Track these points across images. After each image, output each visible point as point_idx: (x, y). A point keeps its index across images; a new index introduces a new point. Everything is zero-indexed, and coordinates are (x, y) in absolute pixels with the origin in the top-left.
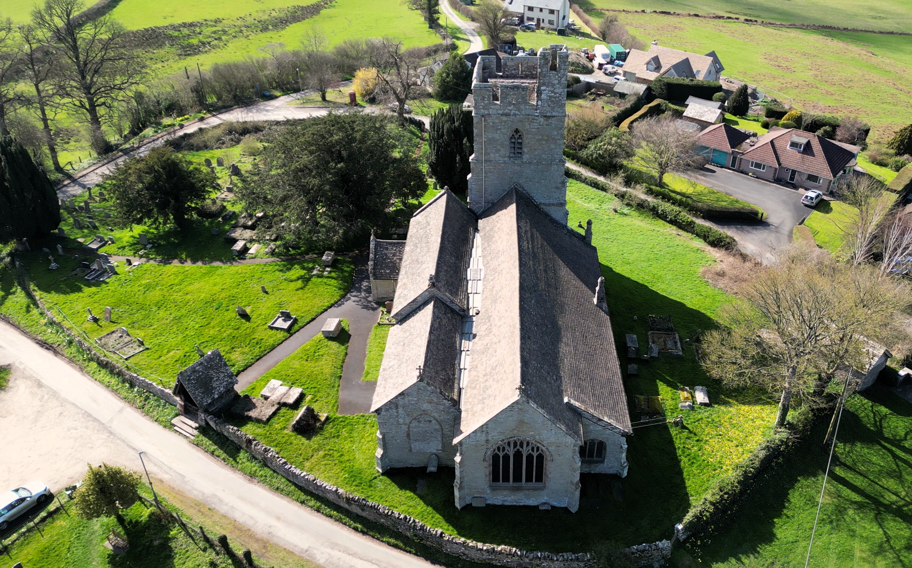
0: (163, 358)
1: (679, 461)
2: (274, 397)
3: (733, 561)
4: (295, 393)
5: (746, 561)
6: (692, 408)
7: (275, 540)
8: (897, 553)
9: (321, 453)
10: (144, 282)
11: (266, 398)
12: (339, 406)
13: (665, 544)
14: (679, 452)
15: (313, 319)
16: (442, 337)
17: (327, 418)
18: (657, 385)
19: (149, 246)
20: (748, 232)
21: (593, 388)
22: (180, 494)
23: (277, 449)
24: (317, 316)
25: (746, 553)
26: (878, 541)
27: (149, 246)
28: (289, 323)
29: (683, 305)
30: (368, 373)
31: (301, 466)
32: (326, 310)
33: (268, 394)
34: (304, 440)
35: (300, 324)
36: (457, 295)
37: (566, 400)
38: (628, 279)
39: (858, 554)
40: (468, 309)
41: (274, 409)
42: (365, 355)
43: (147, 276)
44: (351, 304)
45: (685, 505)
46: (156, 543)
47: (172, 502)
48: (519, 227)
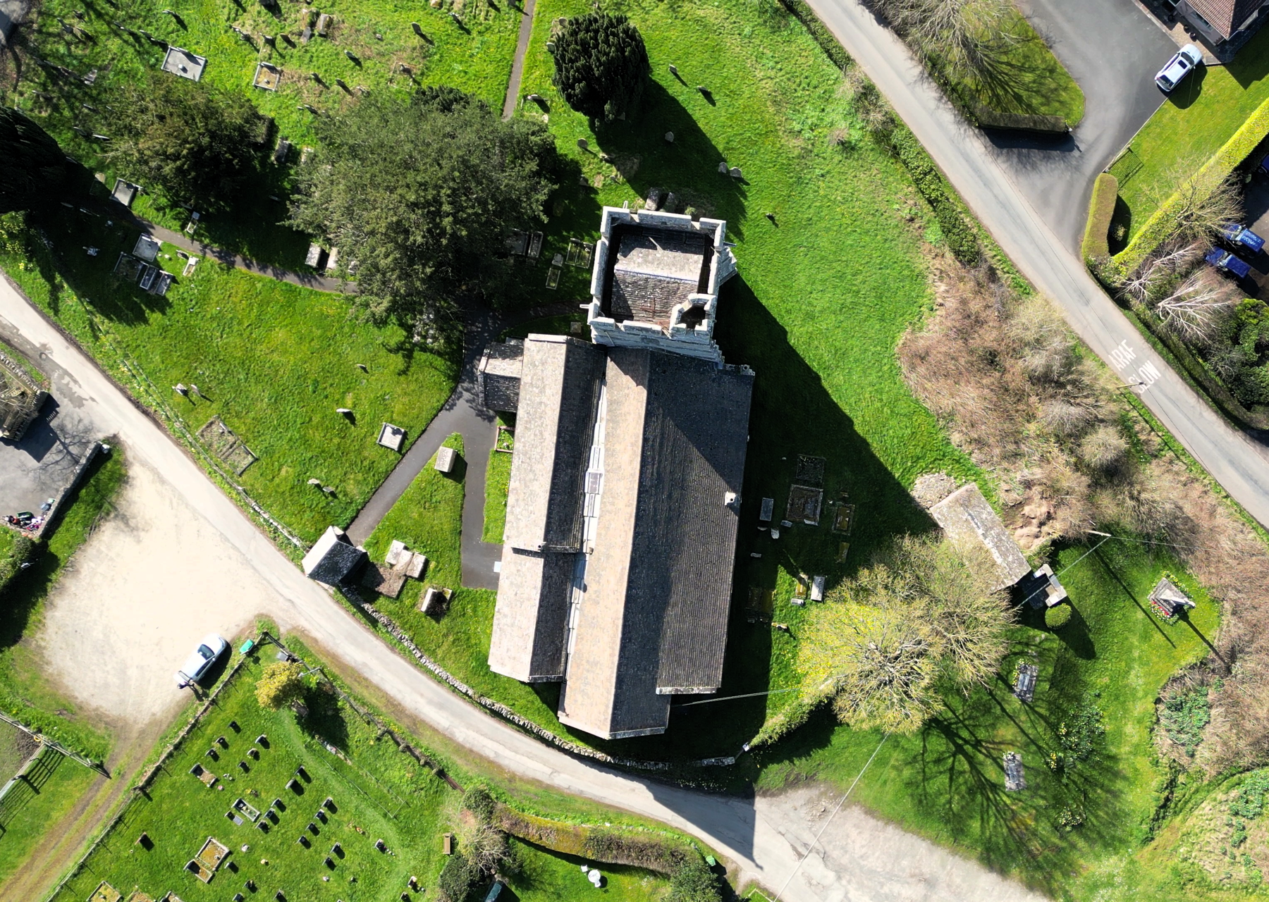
0: (277, 480)
1: (769, 671)
2: (399, 568)
3: (787, 762)
4: (420, 560)
5: (797, 762)
6: (803, 605)
7: (422, 716)
8: (925, 764)
9: (451, 638)
10: (215, 310)
11: (392, 566)
13: (730, 761)
15: (424, 431)
16: (552, 601)
17: (453, 594)
18: (776, 572)
19: (196, 216)
20: (1034, 167)
21: (692, 650)
22: (334, 658)
23: (411, 633)
24: (428, 425)
25: (799, 757)
26: (914, 753)
27: (196, 216)
28: (399, 437)
29: (849, 422)
31: (433, 653)
32: (436, 415)
33: (393, 562)
36: (570, 530)
37: (658, 692)
38: (800, 362)
39: (892, 762)
42: (483, 500)
44: (462, 406)
45: (761, 720)
46: (330, 713)
47: (332, 669)
48: (645, 440)
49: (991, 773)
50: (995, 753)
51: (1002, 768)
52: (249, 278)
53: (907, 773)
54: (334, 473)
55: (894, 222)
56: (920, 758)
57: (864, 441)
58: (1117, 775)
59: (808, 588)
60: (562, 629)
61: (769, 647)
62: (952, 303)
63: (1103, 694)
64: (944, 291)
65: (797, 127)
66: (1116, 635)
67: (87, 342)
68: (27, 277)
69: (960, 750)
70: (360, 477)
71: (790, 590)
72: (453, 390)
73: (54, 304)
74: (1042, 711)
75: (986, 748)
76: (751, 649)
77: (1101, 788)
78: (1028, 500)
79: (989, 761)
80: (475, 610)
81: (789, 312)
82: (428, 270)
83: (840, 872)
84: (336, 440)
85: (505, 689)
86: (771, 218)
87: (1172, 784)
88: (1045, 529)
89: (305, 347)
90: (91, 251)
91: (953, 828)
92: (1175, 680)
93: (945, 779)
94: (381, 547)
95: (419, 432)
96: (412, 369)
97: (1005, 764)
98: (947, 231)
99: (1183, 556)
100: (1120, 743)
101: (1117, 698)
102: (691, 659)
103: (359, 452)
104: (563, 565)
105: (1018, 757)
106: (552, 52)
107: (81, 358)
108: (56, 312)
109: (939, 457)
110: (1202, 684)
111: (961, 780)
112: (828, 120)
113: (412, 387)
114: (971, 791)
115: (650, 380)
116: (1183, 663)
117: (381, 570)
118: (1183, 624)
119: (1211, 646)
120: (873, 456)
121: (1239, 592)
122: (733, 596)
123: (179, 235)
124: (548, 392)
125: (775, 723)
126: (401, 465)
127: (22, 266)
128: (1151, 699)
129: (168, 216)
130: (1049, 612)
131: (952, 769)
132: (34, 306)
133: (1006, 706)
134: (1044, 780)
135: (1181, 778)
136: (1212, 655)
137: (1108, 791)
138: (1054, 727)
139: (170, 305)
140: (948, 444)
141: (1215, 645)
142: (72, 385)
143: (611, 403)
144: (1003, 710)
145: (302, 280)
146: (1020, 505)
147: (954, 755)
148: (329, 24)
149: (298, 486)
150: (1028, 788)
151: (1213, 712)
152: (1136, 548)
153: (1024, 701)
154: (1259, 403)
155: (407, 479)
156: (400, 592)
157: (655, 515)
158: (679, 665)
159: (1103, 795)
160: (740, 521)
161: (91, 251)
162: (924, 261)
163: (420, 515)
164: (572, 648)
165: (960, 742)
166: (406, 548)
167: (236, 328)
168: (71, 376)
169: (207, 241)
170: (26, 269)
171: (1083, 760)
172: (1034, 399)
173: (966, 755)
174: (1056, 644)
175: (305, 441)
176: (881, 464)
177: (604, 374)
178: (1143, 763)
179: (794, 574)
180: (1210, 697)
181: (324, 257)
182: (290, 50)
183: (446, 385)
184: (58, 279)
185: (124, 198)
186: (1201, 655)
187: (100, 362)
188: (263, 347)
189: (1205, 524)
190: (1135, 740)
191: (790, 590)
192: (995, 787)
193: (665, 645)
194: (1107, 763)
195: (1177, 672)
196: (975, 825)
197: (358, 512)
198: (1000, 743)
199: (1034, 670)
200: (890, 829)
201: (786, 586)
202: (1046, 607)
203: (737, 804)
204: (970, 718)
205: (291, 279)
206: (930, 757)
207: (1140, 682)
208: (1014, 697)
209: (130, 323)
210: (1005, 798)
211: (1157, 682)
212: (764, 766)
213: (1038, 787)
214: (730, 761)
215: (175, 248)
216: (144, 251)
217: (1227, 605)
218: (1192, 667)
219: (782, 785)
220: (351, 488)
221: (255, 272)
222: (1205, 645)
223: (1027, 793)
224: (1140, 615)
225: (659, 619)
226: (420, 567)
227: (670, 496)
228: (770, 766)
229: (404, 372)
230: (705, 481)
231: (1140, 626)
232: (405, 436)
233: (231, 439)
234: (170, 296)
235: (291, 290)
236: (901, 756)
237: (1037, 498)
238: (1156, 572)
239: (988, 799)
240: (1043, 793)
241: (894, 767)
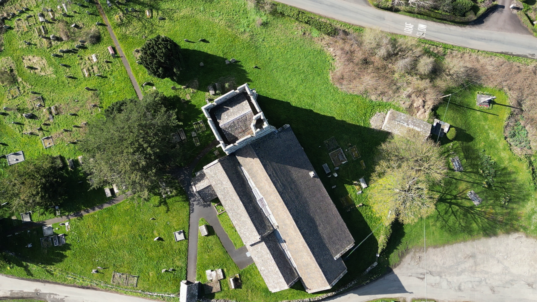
0: (151, 279)
2: (214, 279)
4: (220, 271)
5: (398, 248)
6: (362, 192)
8: (442, 217)
9: (250, 291)
10: (87, 236)
11: (211, 280)
12: (239, 265)
13: (375, 264)
14: (365, 218)
15: (189, 226)
17: (239, 275)
18: (345, 188)
19: (57, 208)
23: (235, 299)
24: (189, 223)
25: (398, 245)
26: (436, 216)
28: (182, 234)
29: (333, 118)
30: (236, 244)
34: (240, 290)
35: (187, 232)
36: (265, 225)
37: (335, 259)
38: (301, 109)
39: (431, 224)
40: (272, 226)
41: (219, 284)
43: (83, 231)
48: (270, 176)
49: (467, 204)
50: (464, 196)
51: (469, 199)
52: (91, 216)
53: (438, 224)
54: (168, 262)
55: (299, 39)
56: (439, 216)
57: (343, 121)
58: (510, 174)
59: (360, 185)
60: (287, 261)
61: (361, 215)
62: (339, 53)
63: (486, 149)
64: (333, 51)
65: (243, 30)
66: (475, 126)
67: (50, 278)
68: (13, 271)
69: (451, 204)
70: (178, 257)
71: (354, 191)
72: (189, 204)
73: (29, 273)
74: (470, 170)
75: (459, 197)
76: (356, 221)
77: (508, 182)
78: (413, 102)
79: (463, 200)
80: (251, 275)
81: (285, 95)
82: (154, 171)
83: (440, 275)
84: (161, 251)
85: (281, 295)
86: (256, 67)
87: (531, 163)
88: (426, 107)
89: (127, 226)
90: (29, 246)
91: (468, 232)
92: (506, 127)
93: (453, 217)
94: (203, 276)
95: (187, 227)
96: (170, 207)
97: (470, 197)
98: (319, 29)
99: (479, 83)
100: (503, 162)
101: (491, 147)
102: (338, 239)
103: (172, 249)
104: (272, 239)
105: (472, 192)
106: (141, 64)
107: (52, 285)
108: (32, 275)
109: (373, 108)
110: (516, 121)
111: (458, 213)
112: (251, 20)
113: (174, 213)
114: (465, 215)
115: (257, 154)
116: (505, 119)
117: (209, 284)
118: (495, 106)
119: (510, 106)
120: (349, 124)
121: (506, 81)
122: (337, 207)
123: (56, 218)
124: (224, 183)
125: (382, 240)
126: (190, 243)
127: (8, 268)
128: (503, 139)
129: (47, 214)
130: (448, 135)
131: (453, 212)
132: (22, 279)
133: (456, 177)
134: (487, 193)
135: (532, 159)
136: (513, 109)
137: (511, 181)
138: (477, 173)
139: (70, 245)
140: (372, 101)
141: (511, 105)
142: (55, 297)
143: (248, 171)
144: (456, 179)
145: (110, 203)
146: (411, 105)
147: (450, 207)
148: (56, 109)
149: (159, 276)
150: (483, 200)
151: (527, 128)
152: (461, 91)
153: (461, 171)
154: (467, 12)
155: (195, 246)
156: (221, 287)
157: (291, 199)
158: (336, 244)
159: (510, 184)
160: (321, 179)
161: (29, 246)
162: (319, 45)
163: (209, 256)
164: (295, 265)
165: (449, 201)
166: (212, 271)
167: (98, 237)
168: (53, 294)
169: (67, 214)
170: (11, 268)
171: (495, 177)
172: (390, 65)
173: (454, 204)
174: (458, 144)
175: (151, 259)
176: (354, 125)
177: (239, 163)
178: (516, 163)
179: (352, 184)
180: (522, 124)
181: (112, 190)
182: (49, 127)
183: (186, 204)
184: (24, 263)
185: (27, 219)
186: (509, 112)
187: (59, 282)
188: (113, 236)
189: (478, 66)
190: (507, 157)
191: (354, 191)
192: (472, 208)
193: (326, 241)
194: (503, 172)
195: (505, 123)
196: (474, 225)
197: (186, 270)
198: (463, 191)
199: (457, 158)
200: (446, 247)
201: (352, 190)
202: (445, 134)
203: (389, 277)
204: (447, 190)
205: (106, 206)
206: (442, 213)
207: (495, 136)
208: (457, 172)
209: (61, 261)
210: (478, 209)
211: (501, 132)
212: (388, 257)
213: (486, 197)
214: (375, 264)
215: (58, 224)
216: (48, 233)
217: (505, 89)
218: (509, 118)
219: (399, 259)
220: (178, 263)
221: (92, 212)
222: (508, 108)
223: (484, 202)
224: (479, 113)
225: (318, 233)
226: (221, 274)
227: (291, 189)
228: (390, 256)
229: (168, 210)
230: (299, 174)
231: (481, 117)
232: (184, 232)
233: (124, 276)
234: (68, 242)
235: (108, 210)
236: (433, 220)
237: (416, 99)
238: (473, 94)
239: (472, 213)
240: (490, 198)
241: (433, 225)
